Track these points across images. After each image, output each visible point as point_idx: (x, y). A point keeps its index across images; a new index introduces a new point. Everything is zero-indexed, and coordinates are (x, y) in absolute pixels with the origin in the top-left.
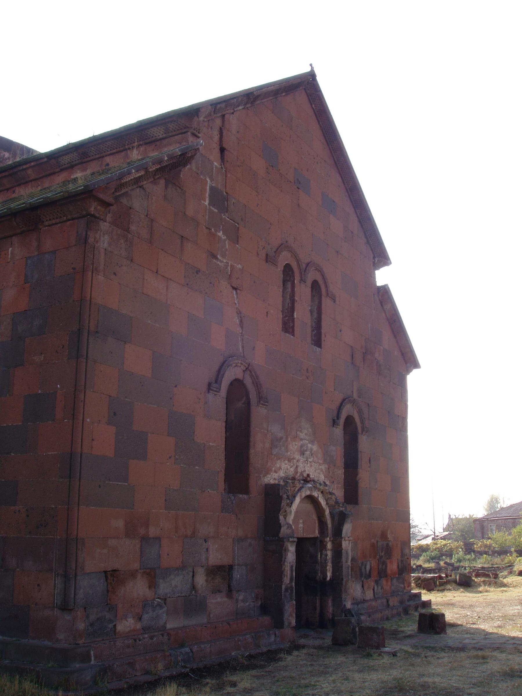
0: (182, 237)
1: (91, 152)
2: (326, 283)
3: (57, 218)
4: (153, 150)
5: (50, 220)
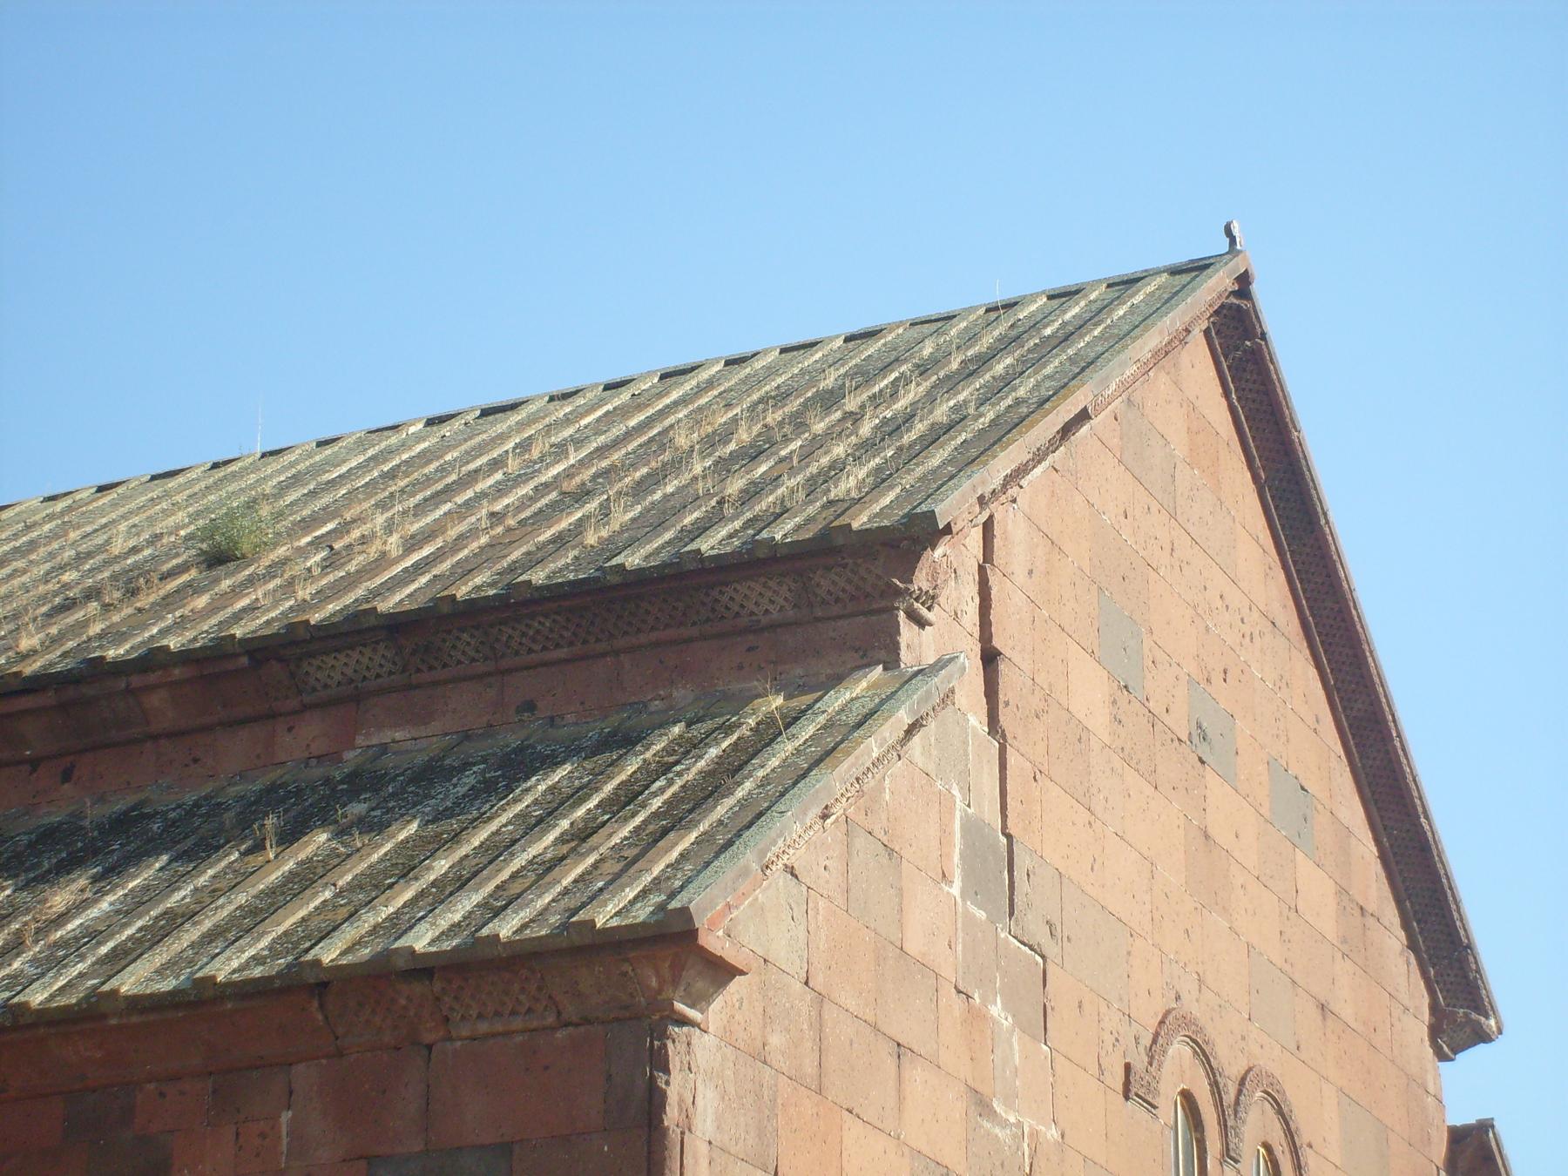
0: (899, 1045)
1: (454, 647)
2: (1295, 1151)
3: (513, 1013)
4: (740, 667)
5: (480, 1016)
